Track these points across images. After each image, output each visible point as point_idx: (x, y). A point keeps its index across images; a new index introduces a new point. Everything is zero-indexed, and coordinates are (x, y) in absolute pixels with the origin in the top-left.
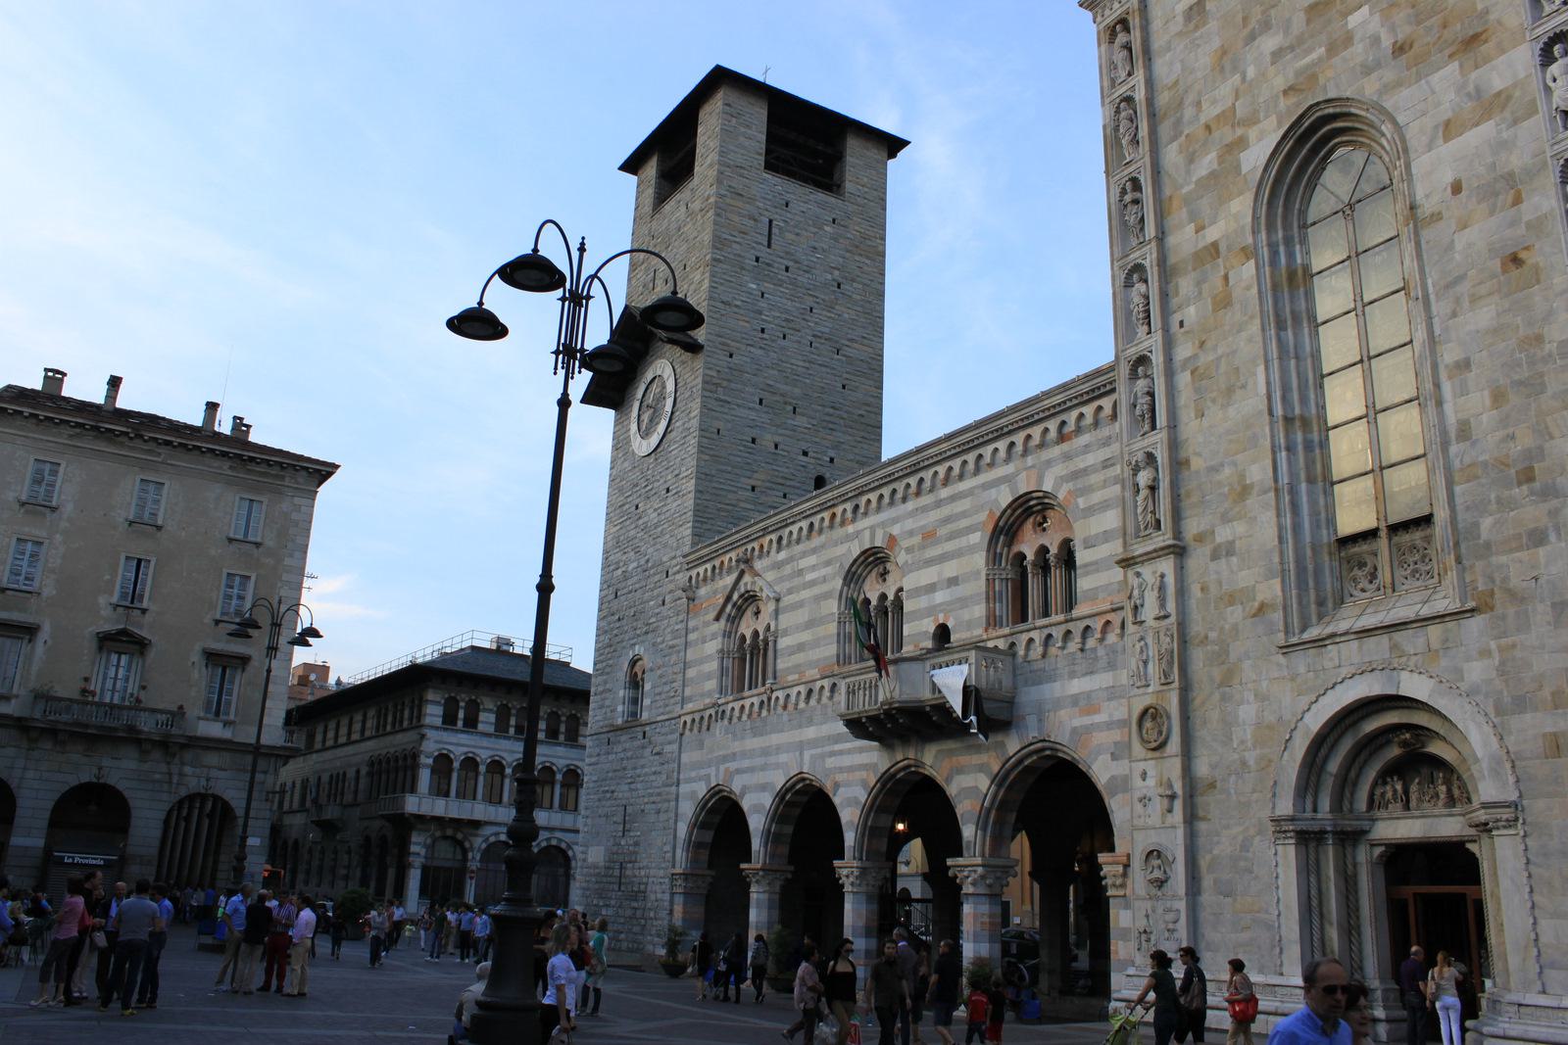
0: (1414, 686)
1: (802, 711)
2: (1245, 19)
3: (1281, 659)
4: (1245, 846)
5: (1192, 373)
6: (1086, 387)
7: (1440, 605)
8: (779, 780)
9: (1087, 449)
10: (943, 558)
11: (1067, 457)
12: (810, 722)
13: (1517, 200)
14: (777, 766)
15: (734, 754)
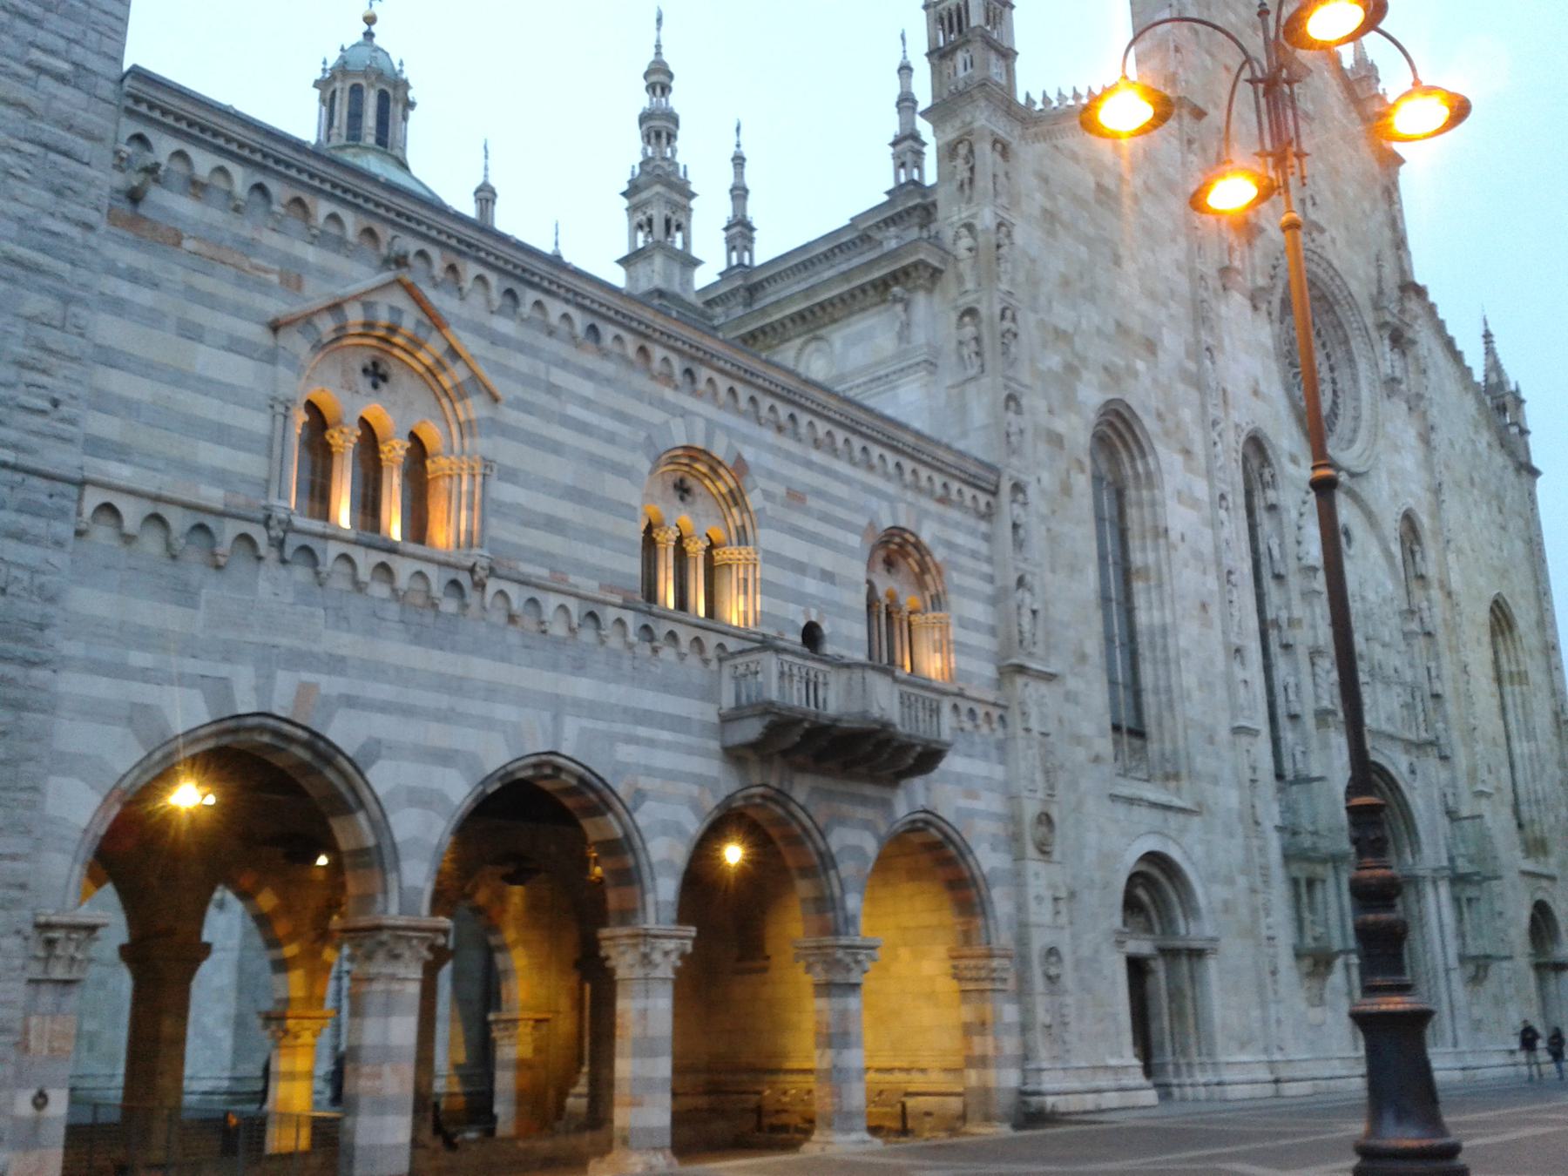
0: (1175, 853)
1: (558, 642)
2: (1081, 276)
3: (1108, 803)
4: (1097, 951)
5: (1049, 530)
6: (973, 469)
7: (1177, 802)
8: (496, 755)
9: (957, 526)
10: (813, 538)
11: (942, 520)
12: (579, 668)
13: (1204, 572)
14: (488, 724)
15: (343, 659)
